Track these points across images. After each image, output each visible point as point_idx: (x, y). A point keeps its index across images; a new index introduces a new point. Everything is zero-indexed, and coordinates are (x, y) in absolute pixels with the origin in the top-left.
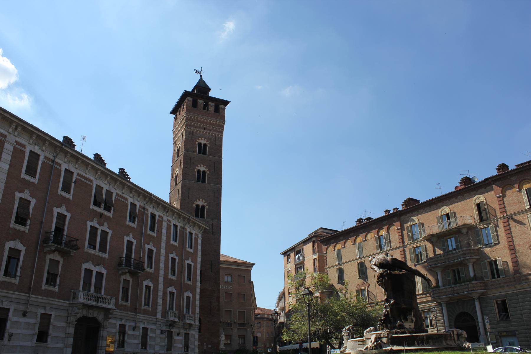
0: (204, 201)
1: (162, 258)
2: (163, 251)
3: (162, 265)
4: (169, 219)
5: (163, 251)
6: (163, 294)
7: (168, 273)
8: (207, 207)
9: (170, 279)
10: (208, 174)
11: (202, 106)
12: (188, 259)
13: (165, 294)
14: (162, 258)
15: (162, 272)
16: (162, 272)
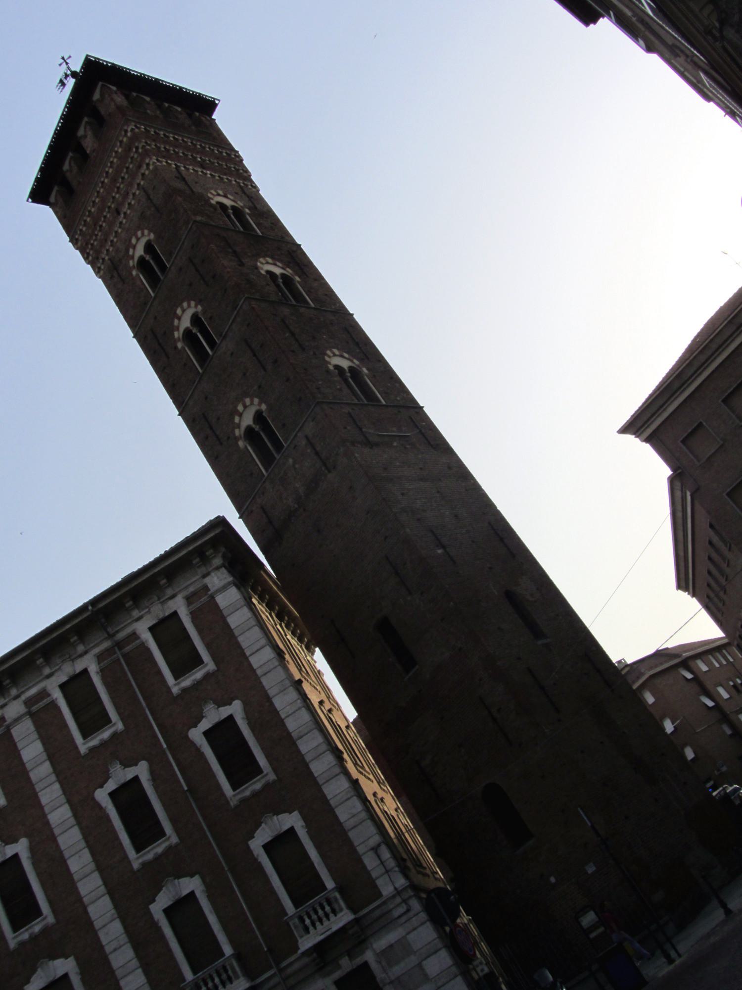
0: (248, 401)
1: (70, 839)
2: (60, 815)
3: (80, 862)
4: (33, 691)
5: (60, 815)
6: (137, 946)
7: (126, 857)
8: (264, 407)
9: (144, 865)
10: (204, 312)
11: (75, 169)
12: (200, 718)
13: (143, 938)
14: (70, 839)
15: (90, 884)
16: (90, 884)
